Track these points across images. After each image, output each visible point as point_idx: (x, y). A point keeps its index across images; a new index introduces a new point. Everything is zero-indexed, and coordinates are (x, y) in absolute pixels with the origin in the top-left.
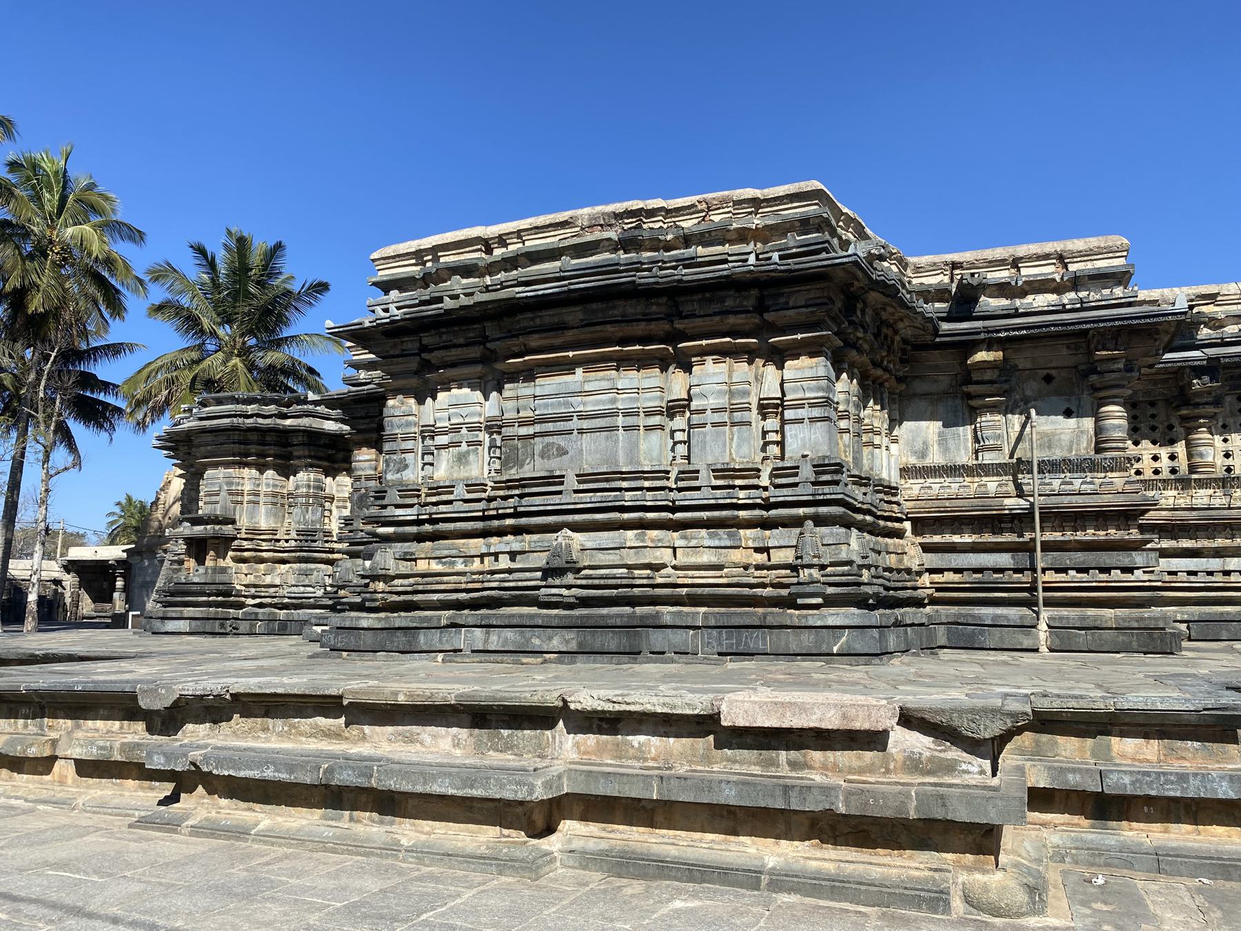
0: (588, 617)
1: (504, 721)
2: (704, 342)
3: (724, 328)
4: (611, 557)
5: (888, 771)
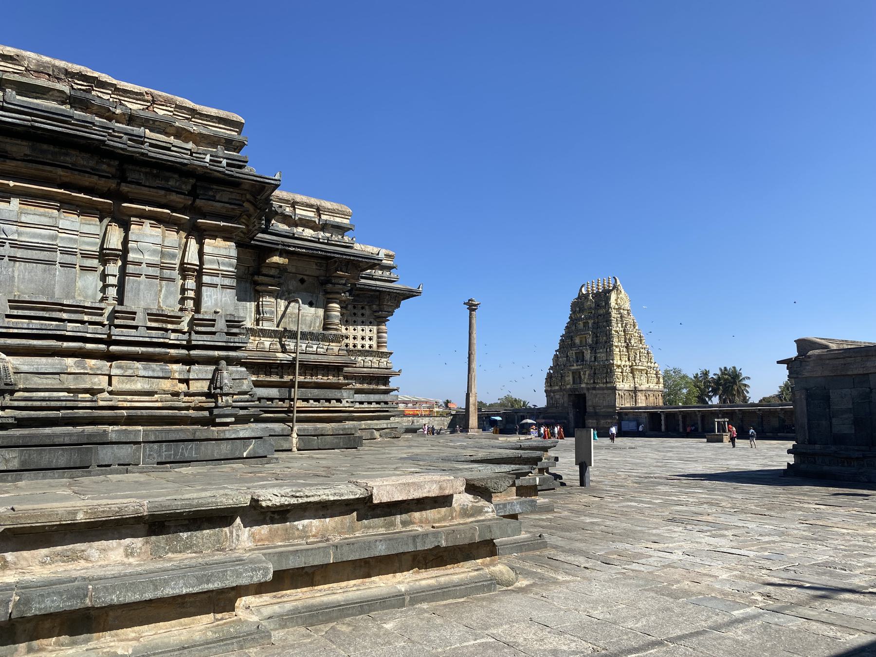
0: (32, 436)
1: (182, 525)
2: (147, 208)
3: (163, 201)
4: (49, 381)
5: (453, 518)
